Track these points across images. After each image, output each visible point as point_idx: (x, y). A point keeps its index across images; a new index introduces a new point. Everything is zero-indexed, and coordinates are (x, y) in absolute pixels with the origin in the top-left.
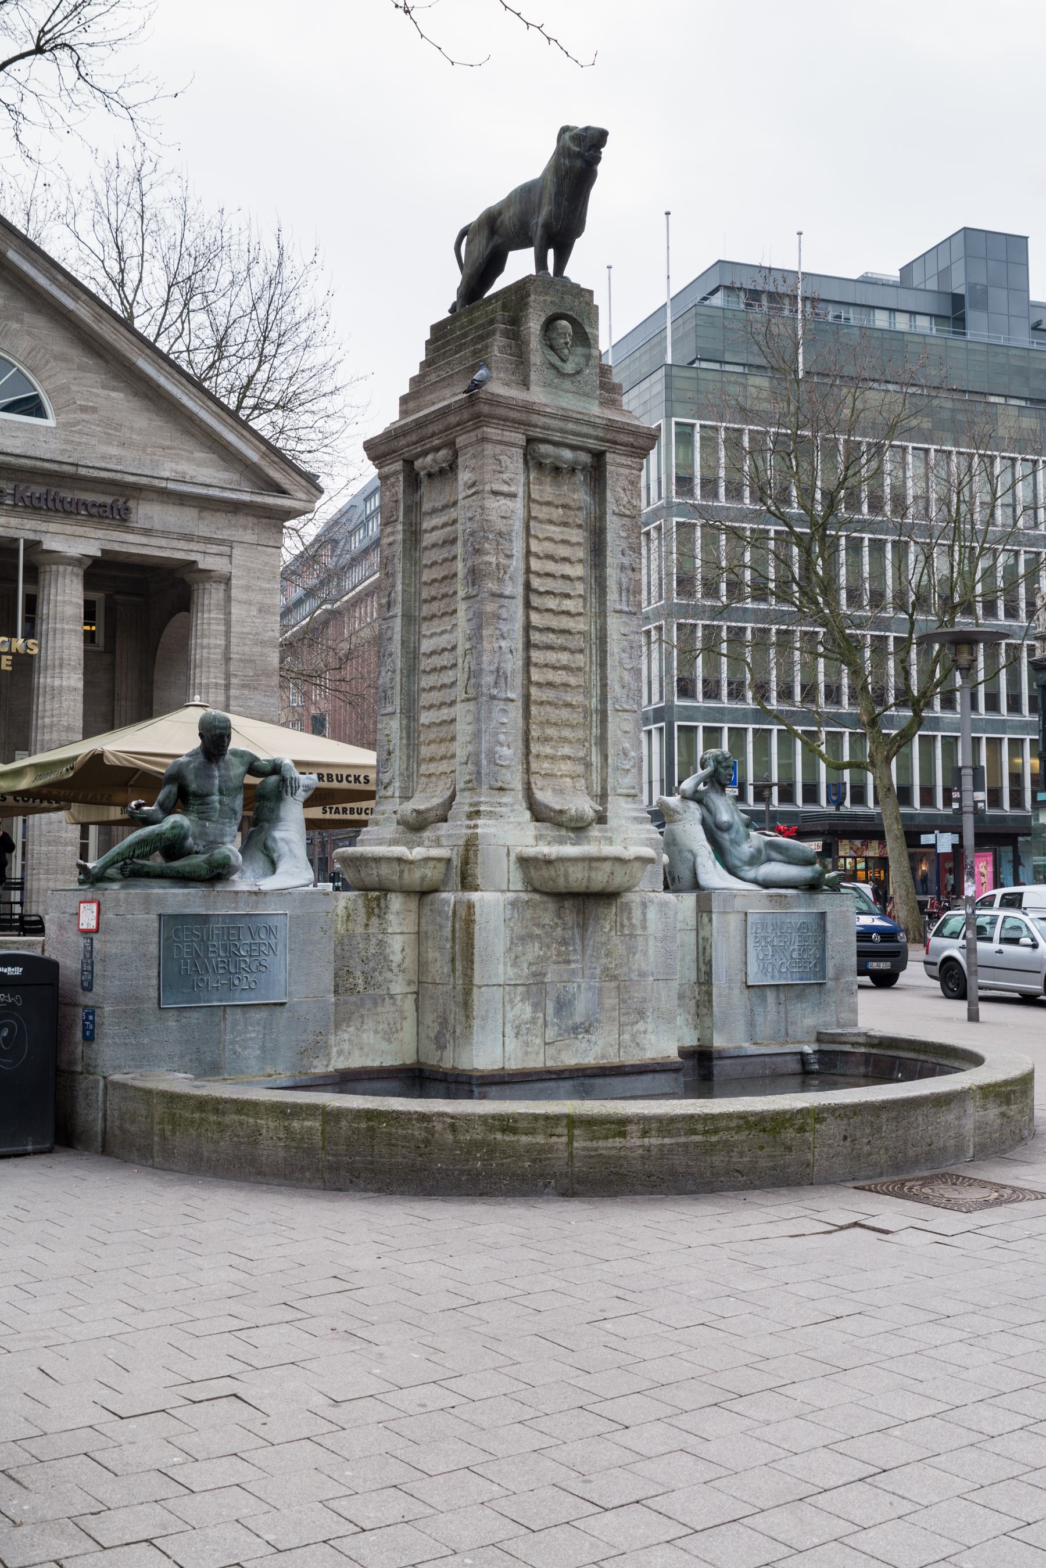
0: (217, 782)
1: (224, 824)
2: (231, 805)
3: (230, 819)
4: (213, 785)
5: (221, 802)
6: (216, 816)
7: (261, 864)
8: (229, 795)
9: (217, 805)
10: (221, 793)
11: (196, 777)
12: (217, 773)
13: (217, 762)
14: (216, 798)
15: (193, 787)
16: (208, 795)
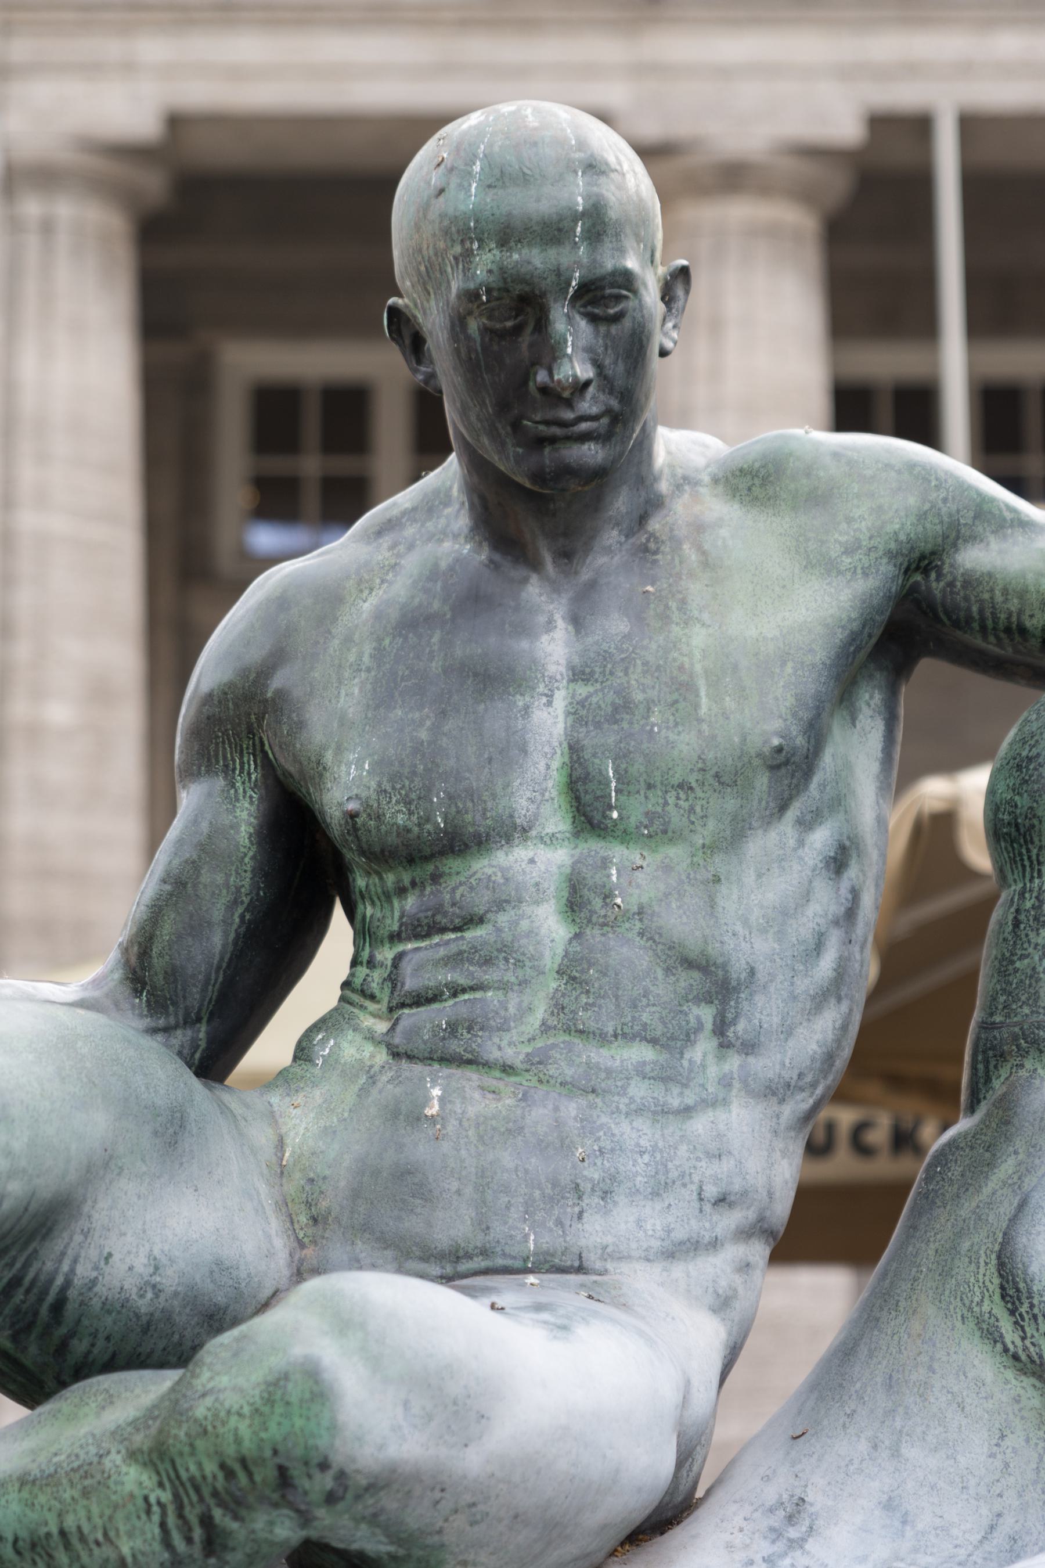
0: (549, 721)
1: (588, 1088)
2: (681, 922)
3: (674, 1040)
4: (511, 751)
5: (577, 899)
6: (522, 1017)
7: (975, 1451)
8: (657, 832)
9: (549, 927)
10: (589, 815)
11: (382, 699)
12: (554, 647)
13: (567, 556)
14: (538, 861)
15: (347, 786)
16: (459, 842)
